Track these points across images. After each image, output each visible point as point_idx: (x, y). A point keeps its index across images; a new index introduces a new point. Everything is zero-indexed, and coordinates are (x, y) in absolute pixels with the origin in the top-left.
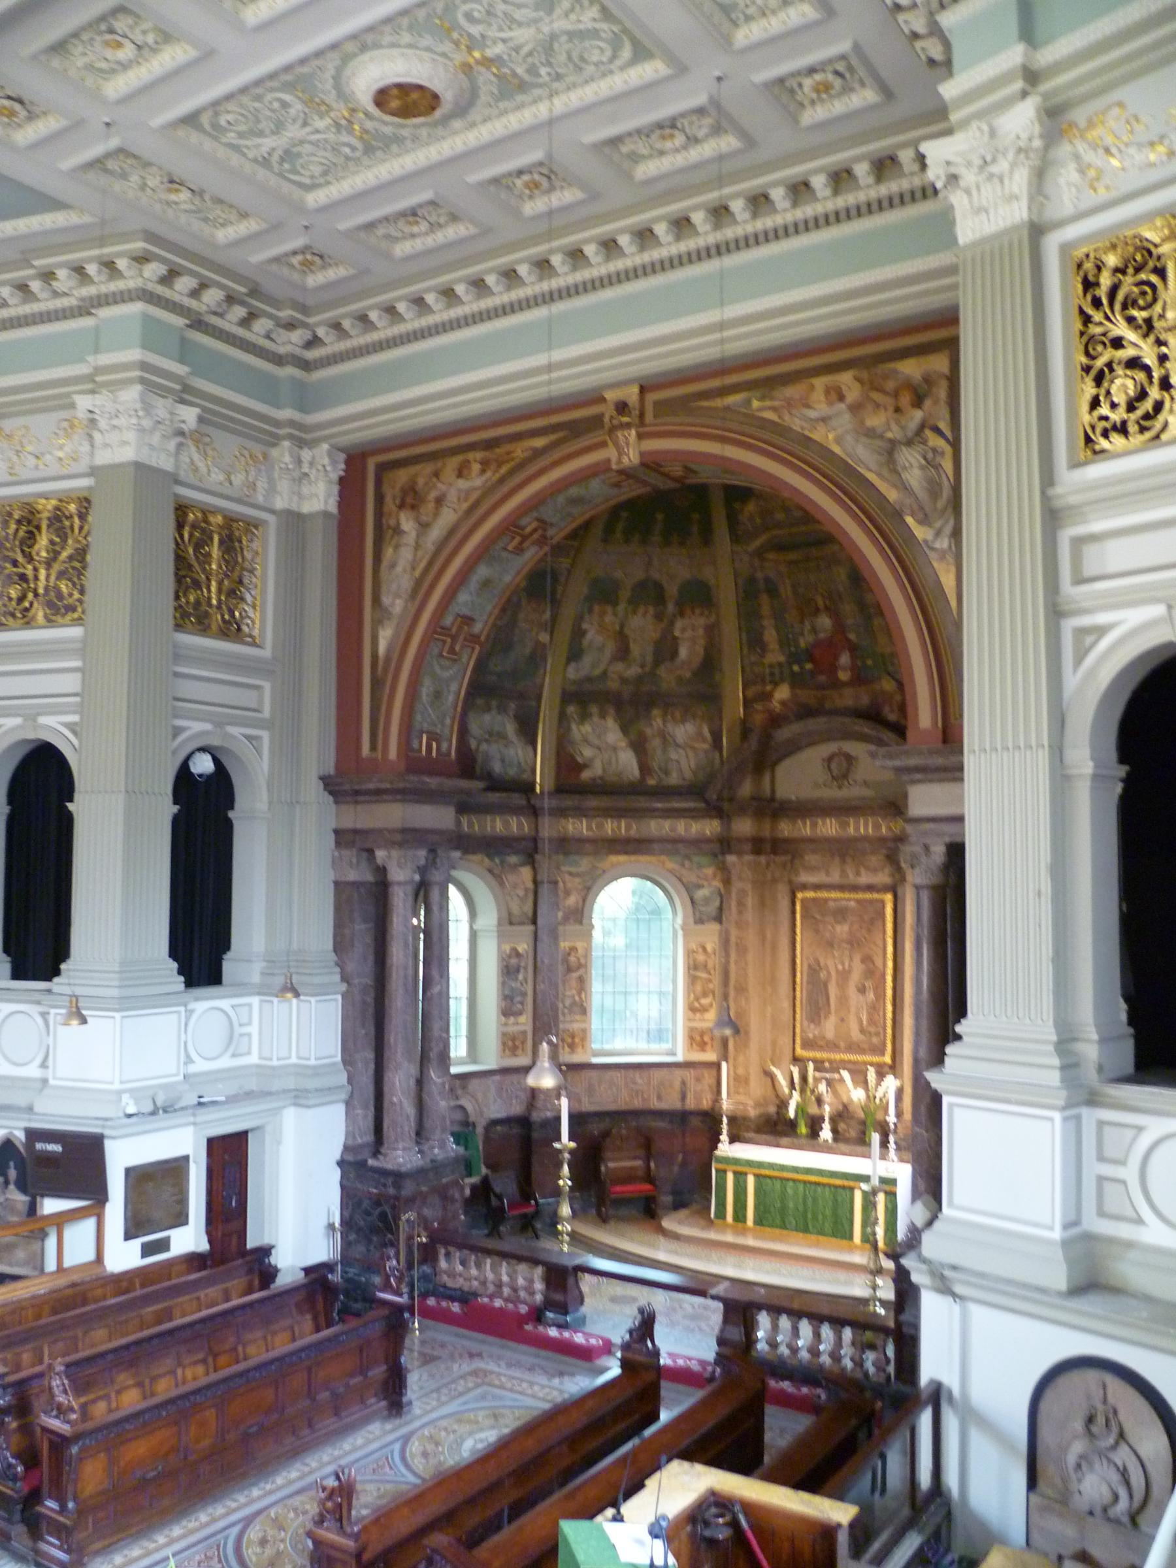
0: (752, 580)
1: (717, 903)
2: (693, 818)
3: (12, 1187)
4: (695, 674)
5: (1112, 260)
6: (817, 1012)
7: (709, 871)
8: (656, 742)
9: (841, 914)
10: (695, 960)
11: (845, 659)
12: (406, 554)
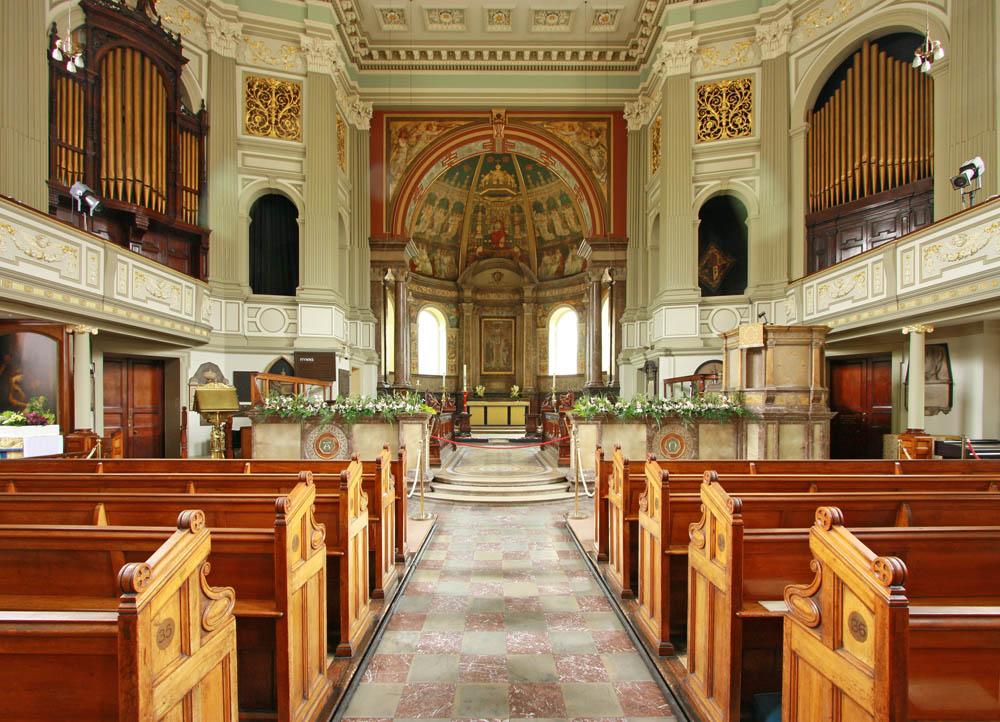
0: (478, 206)
4: (453, 238)
5: (708, 89)
6: (489, 358)
8: (438, 262)
9: (497, 326)
11: (502, 240)
12: (403, 156)
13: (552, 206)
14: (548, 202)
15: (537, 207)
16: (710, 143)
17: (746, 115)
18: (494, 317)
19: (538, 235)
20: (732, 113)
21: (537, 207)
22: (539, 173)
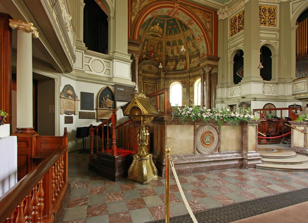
0: (146, 39)
3: (108, 99)
5: (262, 7)
9: (150, 86)
11: (153, 54)
12: (138, 6)
13: (174, 44)
14: (173, 42)
15: (168, 44)
16: (263, 26)
17: (274, 20)
18: (148, 83)
19: (166, 54)
20: (270, 18)
21: (168, 44)
22: (173, 30)
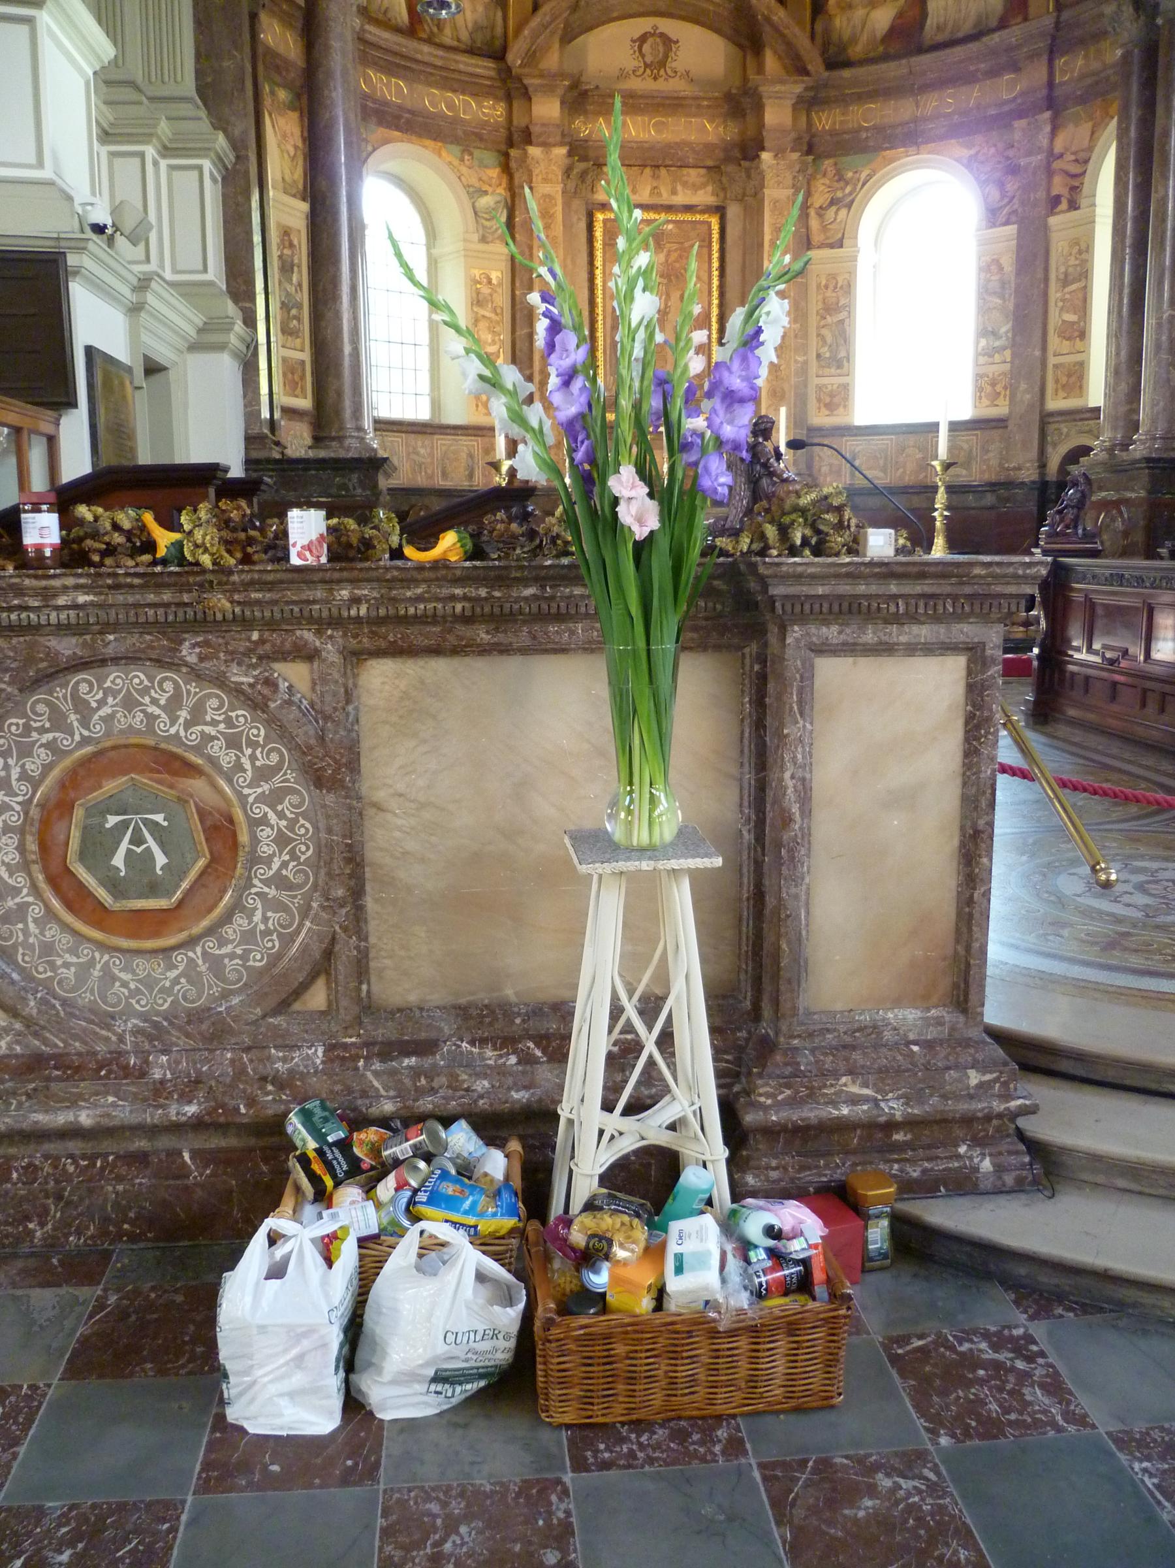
1: (504, 219)
2: (473, 95)
7: (494, 173)
10: (478, 292)
